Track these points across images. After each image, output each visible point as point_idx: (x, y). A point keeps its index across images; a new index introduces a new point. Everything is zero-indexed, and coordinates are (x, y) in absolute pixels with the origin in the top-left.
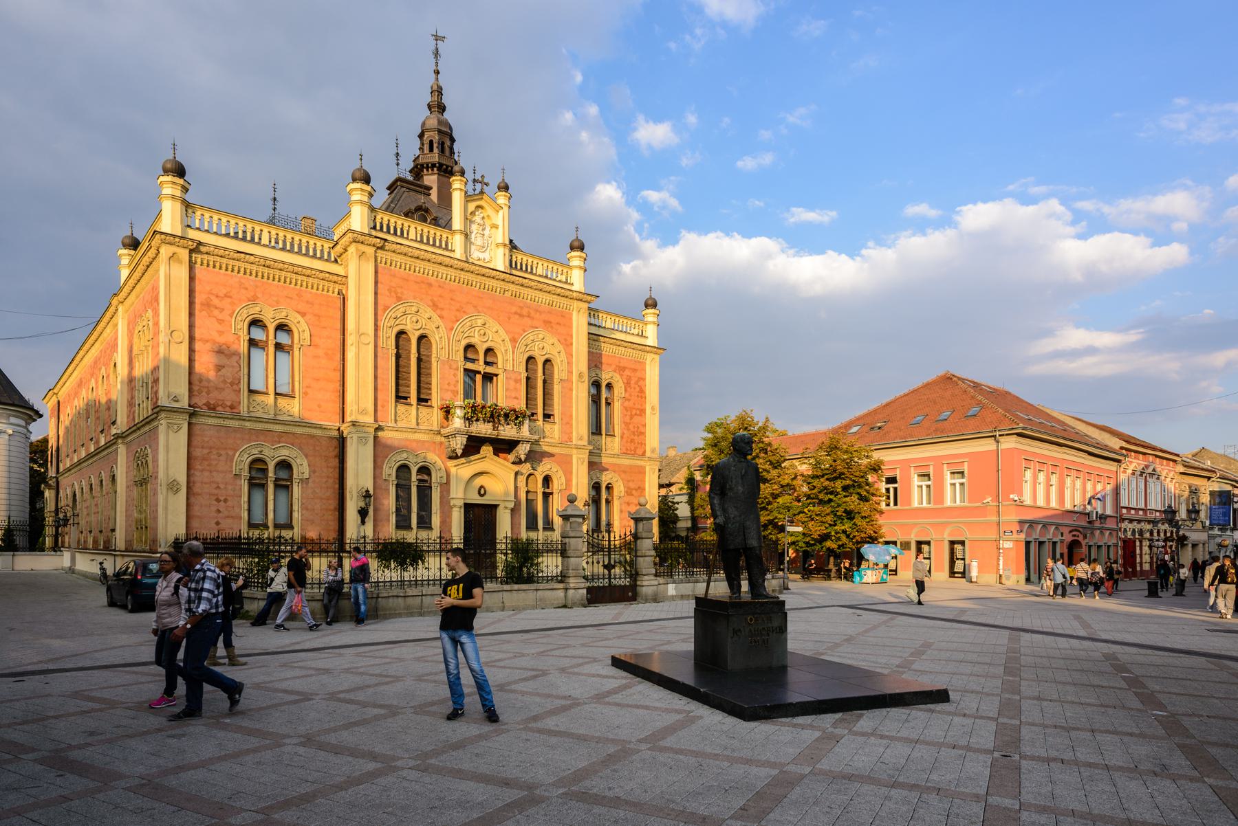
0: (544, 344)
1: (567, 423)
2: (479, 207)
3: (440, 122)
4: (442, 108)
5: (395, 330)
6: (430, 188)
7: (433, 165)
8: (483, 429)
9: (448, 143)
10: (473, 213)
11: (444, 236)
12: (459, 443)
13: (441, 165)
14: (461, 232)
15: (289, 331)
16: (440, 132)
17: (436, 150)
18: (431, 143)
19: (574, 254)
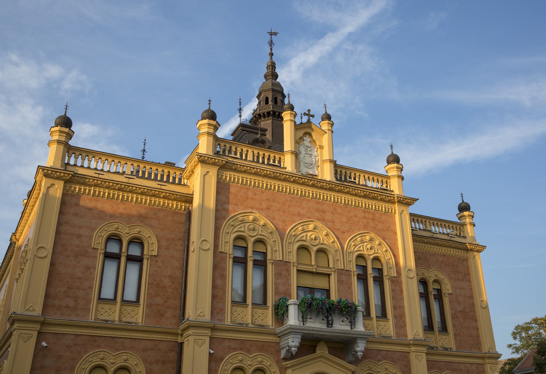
0: (370, 245)
1: (400, 318)
2: (306, 134)
3: (273, 84)
4: (275, 76)
5: (233, 236)
6: (266, 130)
7: (269, 113)
8: (316, 325)
9: (279, 98)
10: (300, 138)
11: (277, 157)
12: (294, 342)
13: (274, 113)
14: (292, 153)
15: (141, 244)
16: (273, 90)
17: (270, 103)
18: (267, 99)
19: (390, 166)
